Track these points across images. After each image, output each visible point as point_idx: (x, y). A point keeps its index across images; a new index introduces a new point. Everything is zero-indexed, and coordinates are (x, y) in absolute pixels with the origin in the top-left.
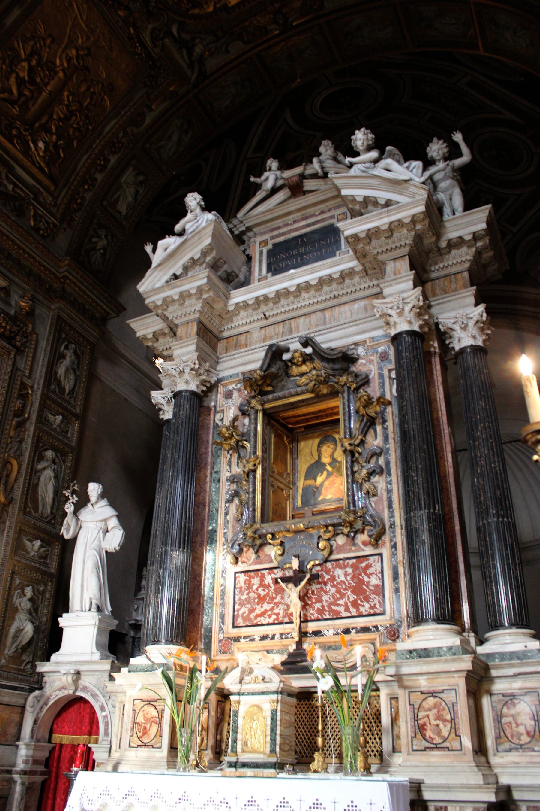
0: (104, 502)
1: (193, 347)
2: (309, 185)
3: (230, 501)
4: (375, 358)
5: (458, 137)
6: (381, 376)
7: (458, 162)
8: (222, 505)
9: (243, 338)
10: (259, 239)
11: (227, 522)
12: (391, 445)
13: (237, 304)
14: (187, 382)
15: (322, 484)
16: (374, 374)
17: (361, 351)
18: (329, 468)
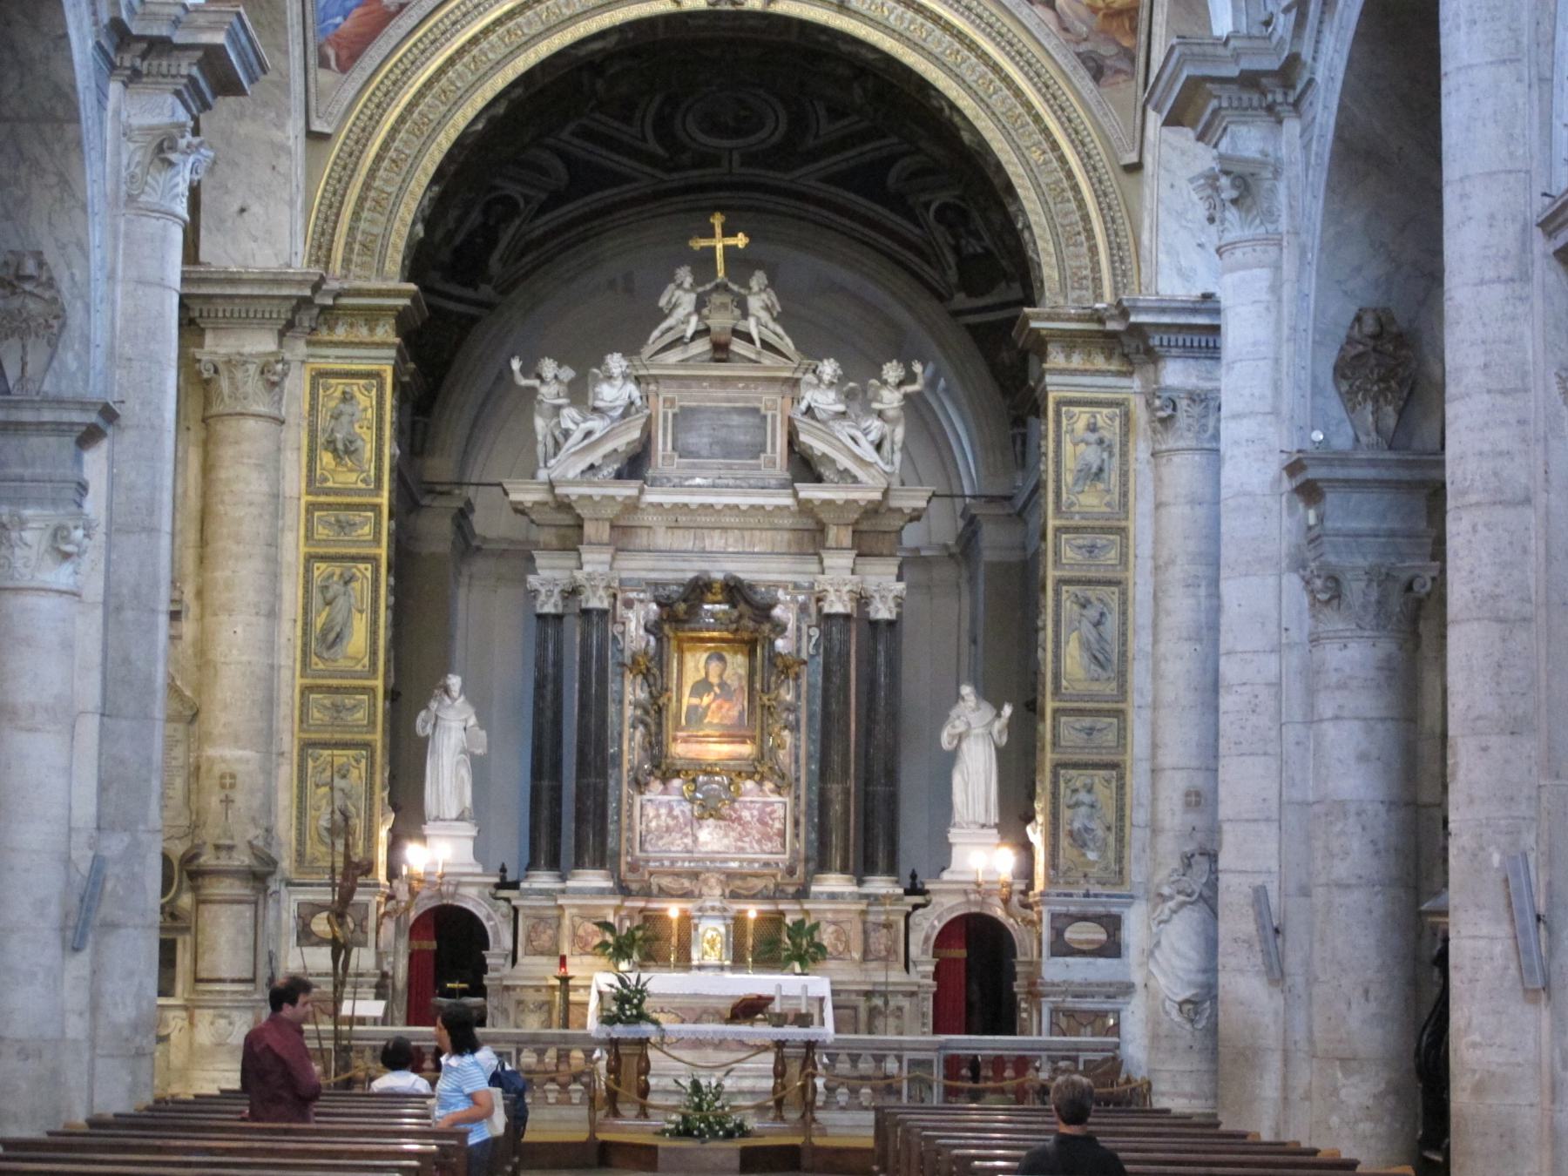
0: (462, 699)
1: (607, 557)
2: (738, 346)
3: (634, 727)
4: (794, 608)
5: (917, 368)
6: (799, 629)
7: (910, 389)
8: (627, 731)
9: (645, 532)
10: (665, 393)
11: (632, 749)
12: (803, 703)
13: (651, 504)
14: (600, 598)
15: (708, 706)
16: (791, 626)
17: (781, 594)
18: (717, 690)
